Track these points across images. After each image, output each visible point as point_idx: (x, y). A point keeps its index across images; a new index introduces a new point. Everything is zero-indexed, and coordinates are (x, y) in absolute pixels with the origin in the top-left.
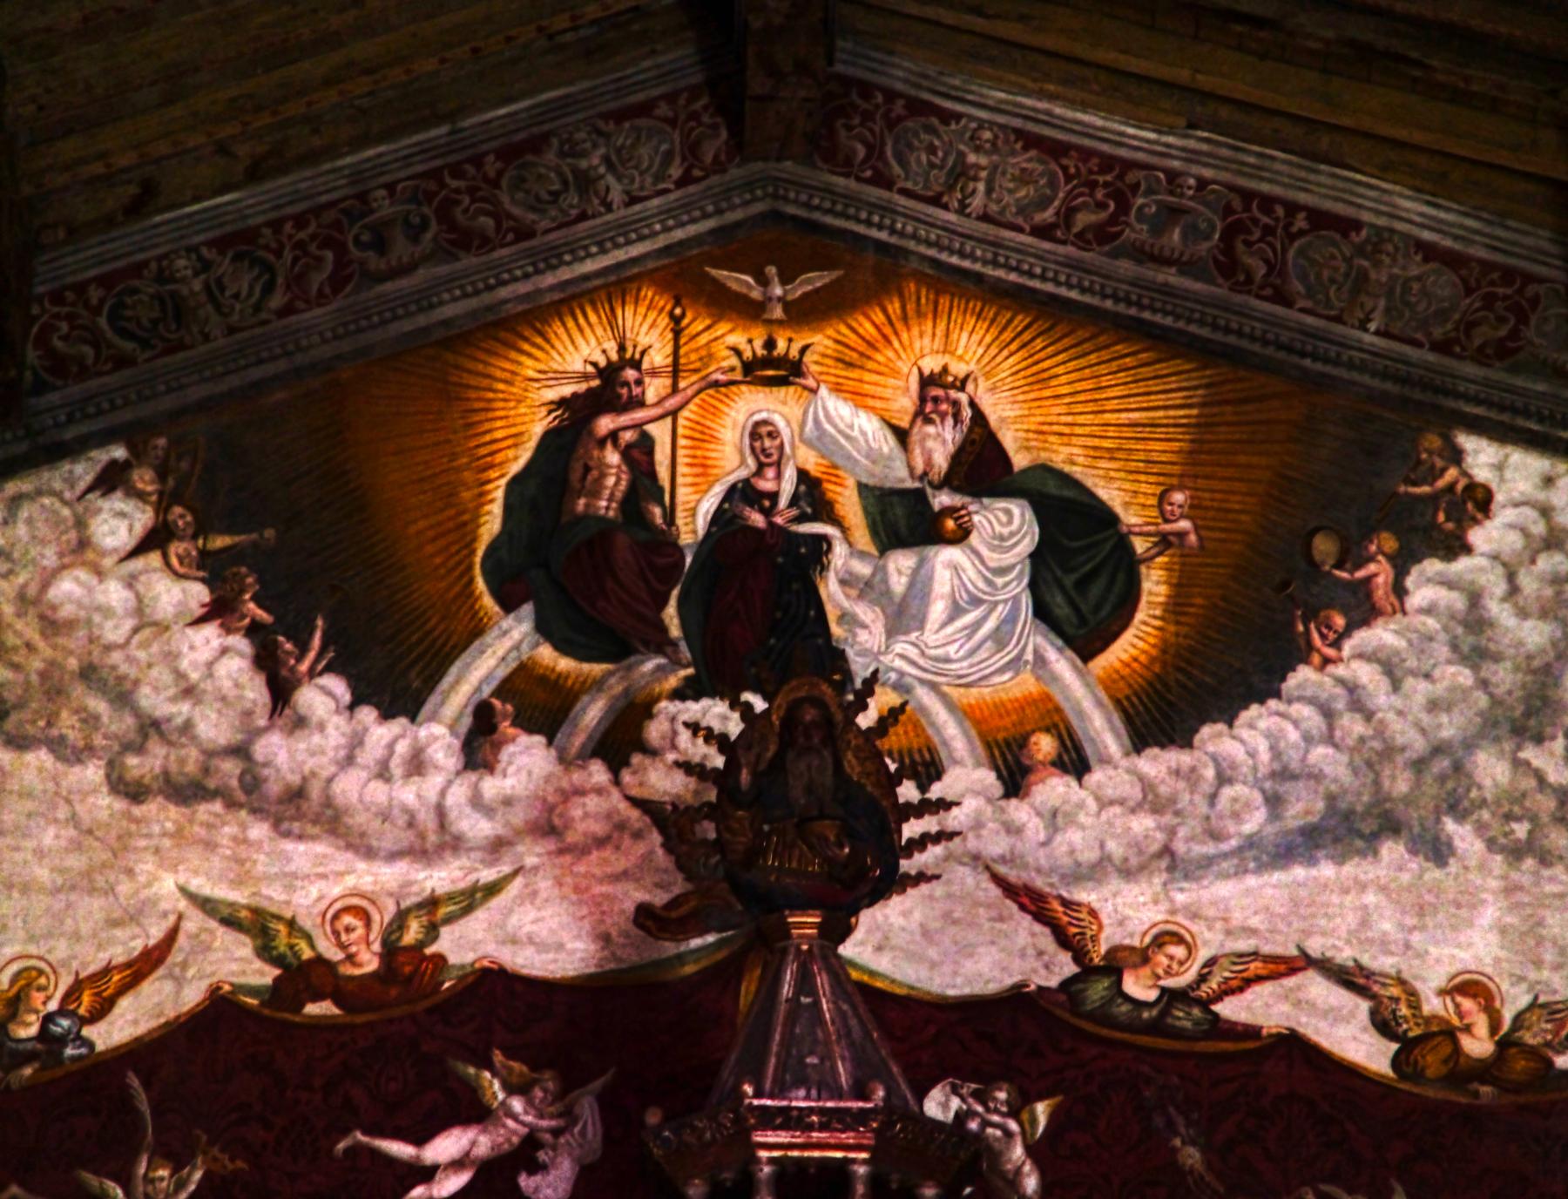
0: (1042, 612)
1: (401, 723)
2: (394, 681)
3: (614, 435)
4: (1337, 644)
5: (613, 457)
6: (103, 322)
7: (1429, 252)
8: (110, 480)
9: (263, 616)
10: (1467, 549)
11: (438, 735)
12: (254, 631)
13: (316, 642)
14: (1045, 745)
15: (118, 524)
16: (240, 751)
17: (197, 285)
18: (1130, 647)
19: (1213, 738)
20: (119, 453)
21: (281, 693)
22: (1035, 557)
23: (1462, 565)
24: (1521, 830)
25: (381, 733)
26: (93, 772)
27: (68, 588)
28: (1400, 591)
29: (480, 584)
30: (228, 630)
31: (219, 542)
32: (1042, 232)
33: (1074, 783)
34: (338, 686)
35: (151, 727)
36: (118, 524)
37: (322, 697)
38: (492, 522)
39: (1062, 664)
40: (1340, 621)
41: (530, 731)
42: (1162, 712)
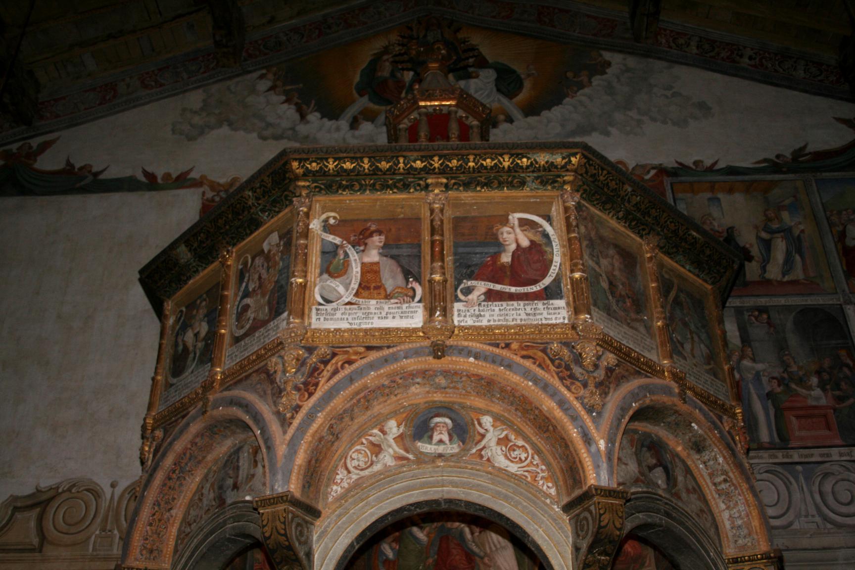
0: (499, 90)
1: (333, 122)
2: (331, 112)
3: (388, 60)
4: (576, 93)
5: (387, 64)
6: (262, 47)
7: (588, 16)
8: (262, 77)
9: (300, 101)
10: (606, 73)
11: (344, 124)
12: (296, 104)
13: (312, 105)
14: (502, 117)
15: (264, 85)
16: (293, 129)
17: (285, 38)
18: (521, 97)
19: (545, 113)
20: (264, 71)
21: (303, 117)
22: (497, 80)
23: (604, 77)
24: (628, 129)
25: (328, 123)
26: (255, 135)
27: (250, 100)
28: (590, 82)
29: (354, 92)
30: (290, 104)
31: (288, 88)
32: (494, 17)
33: (509, 124)
34: (318, 115)
35: (269, 125)
36: (264, 85)
37: (314, 117)
38: (357, 78)
39: (505, 101)
40: (575, 89)
41: (367, 120)
42: (531, 109)
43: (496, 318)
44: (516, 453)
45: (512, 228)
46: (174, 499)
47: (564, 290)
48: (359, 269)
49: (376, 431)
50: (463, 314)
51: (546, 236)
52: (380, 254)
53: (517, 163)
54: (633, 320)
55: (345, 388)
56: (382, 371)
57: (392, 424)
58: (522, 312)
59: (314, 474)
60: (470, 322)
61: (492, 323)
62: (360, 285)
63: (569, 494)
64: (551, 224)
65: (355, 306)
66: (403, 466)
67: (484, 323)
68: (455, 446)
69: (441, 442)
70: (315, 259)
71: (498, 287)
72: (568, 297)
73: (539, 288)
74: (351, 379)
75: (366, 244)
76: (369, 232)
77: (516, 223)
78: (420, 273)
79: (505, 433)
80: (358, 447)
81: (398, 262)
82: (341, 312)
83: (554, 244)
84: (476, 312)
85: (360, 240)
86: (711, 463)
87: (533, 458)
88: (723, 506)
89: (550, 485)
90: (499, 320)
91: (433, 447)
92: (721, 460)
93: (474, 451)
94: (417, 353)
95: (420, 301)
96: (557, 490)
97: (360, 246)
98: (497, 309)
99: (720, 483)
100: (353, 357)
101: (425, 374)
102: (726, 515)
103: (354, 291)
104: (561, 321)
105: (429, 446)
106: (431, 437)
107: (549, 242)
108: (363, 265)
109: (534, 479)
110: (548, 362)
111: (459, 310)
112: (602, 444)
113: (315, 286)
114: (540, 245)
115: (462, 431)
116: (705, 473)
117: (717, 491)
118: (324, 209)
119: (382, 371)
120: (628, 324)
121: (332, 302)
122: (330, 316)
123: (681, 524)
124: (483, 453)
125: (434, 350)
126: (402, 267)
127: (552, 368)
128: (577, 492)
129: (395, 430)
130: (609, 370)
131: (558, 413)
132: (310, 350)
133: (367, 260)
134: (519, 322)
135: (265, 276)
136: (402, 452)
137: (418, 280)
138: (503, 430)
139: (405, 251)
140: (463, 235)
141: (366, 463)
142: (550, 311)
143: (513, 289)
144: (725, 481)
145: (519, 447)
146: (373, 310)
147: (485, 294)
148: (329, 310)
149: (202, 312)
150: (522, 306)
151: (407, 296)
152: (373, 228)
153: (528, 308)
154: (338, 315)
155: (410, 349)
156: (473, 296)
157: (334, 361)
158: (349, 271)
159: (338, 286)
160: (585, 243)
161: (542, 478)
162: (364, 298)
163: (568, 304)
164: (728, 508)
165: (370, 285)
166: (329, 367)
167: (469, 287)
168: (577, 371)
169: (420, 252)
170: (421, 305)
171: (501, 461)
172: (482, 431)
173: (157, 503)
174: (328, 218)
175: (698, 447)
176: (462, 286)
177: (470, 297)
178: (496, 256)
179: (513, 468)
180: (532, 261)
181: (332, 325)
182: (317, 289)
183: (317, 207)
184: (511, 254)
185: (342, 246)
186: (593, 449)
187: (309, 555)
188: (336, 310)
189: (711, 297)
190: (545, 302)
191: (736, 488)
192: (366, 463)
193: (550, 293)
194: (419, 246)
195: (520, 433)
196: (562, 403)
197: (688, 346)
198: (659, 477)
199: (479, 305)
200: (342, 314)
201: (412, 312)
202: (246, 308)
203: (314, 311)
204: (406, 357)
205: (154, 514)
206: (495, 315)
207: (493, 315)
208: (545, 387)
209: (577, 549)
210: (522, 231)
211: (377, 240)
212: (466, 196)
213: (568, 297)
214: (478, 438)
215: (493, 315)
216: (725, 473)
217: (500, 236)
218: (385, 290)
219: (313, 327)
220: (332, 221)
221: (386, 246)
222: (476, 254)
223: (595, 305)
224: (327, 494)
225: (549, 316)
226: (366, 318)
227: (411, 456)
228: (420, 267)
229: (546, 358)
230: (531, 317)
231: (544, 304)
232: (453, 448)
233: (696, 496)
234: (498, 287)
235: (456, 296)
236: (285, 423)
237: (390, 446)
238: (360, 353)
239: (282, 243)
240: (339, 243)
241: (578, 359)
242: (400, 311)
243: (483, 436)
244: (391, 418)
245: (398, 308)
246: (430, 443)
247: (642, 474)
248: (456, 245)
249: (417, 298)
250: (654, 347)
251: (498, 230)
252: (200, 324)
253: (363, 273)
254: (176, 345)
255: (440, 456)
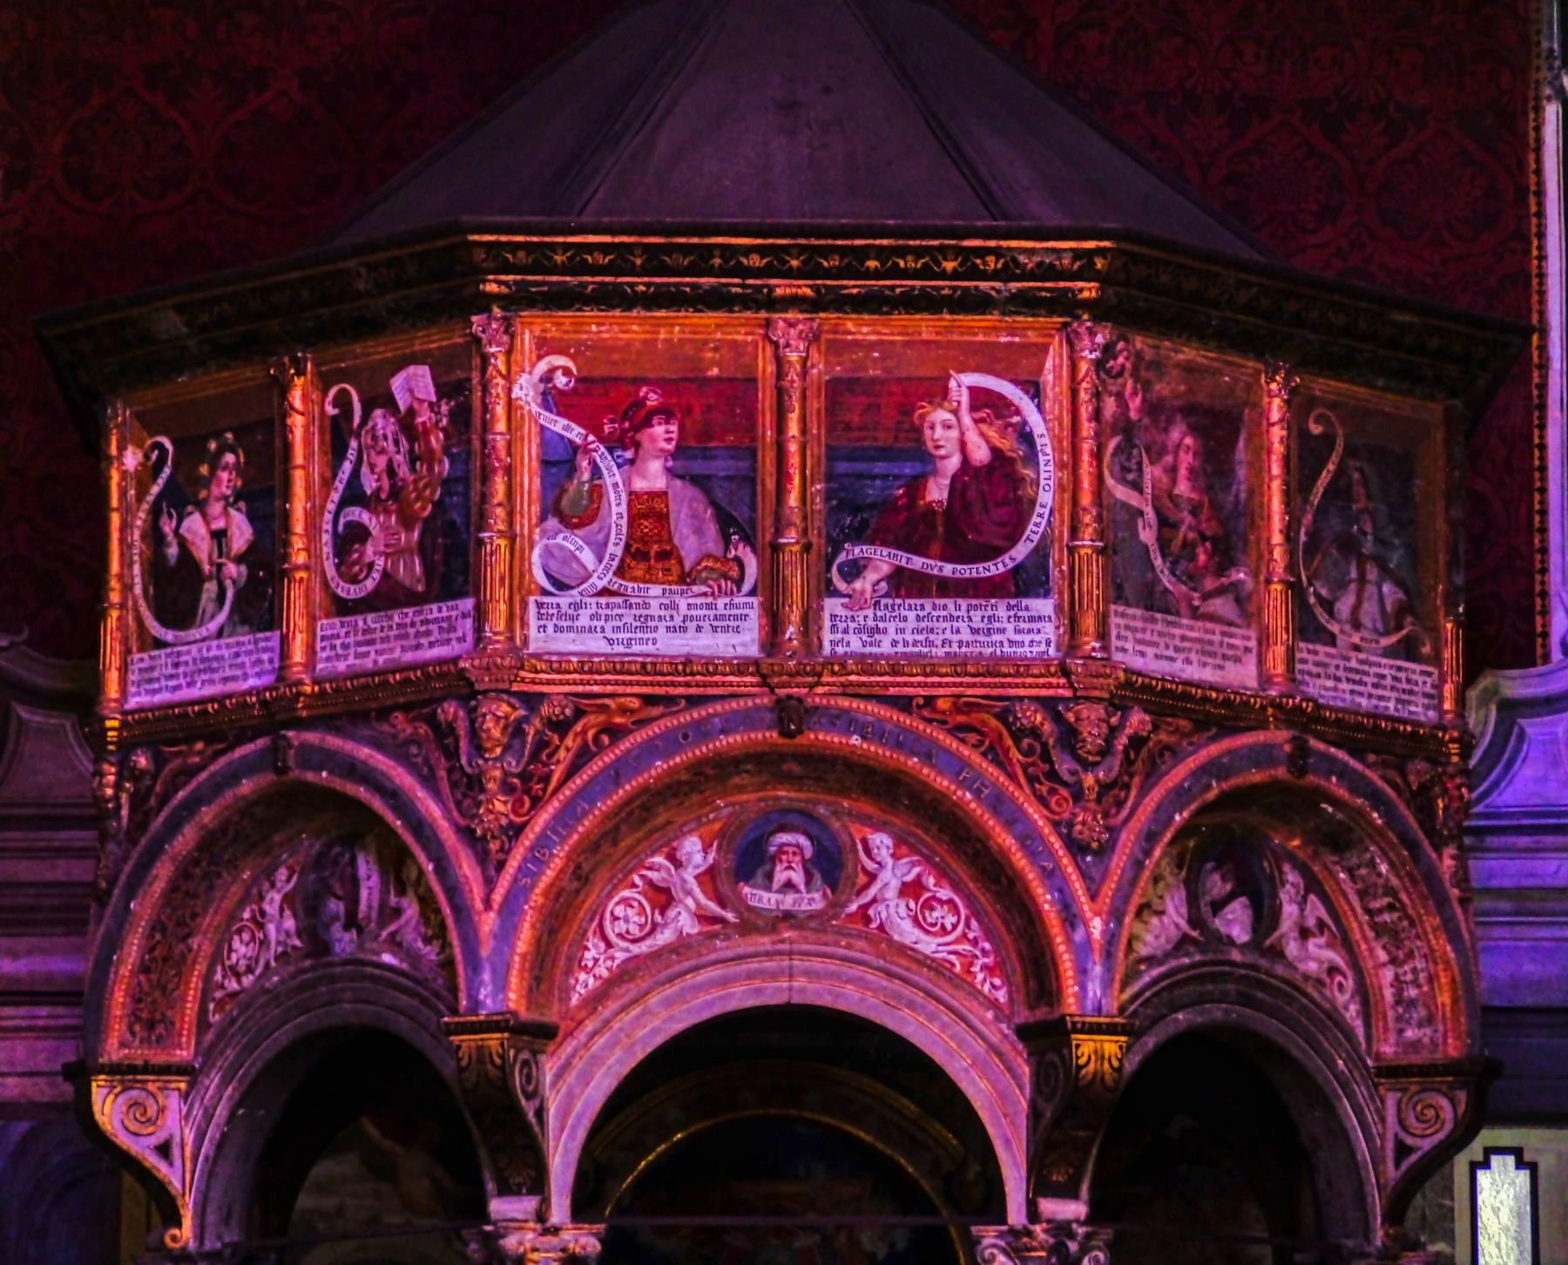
43: (909, 637)
44: (936, 914)
45: (955, 412)
46: (194, 916)
47: (1054, 573)
48: (624, 508)
49: (659, 859)
50: (842, 626)
51: (1027, 438)
52: (668, 470)
53: (976, 265)
54: (1206, 597)
55: (606, 794)
56: (678, 759)
57: (691, 846)
58: (962, 625)
59: (548, 965)
60: (855, 644)
61: (900, 649)
62: (627, 546)
63: (1031, 1008)
64: (1040, 407)
65: (619, 600)
66: (714, 935)
67: (886, 648)
68: (817, 896)
69: (789, 885)
70: (530, 480)
71: (918, 562)
72: (1061, 593)
73: (1001, 569)
74: (616, 774)
75: (637, 445)
76: (643, 413)
77: (965, 399)
78: (753, 522)
79: (917, 870)
80: (626, 893)
81: (707, 492)
82: (589, 612)
83: (1042, 458)
84: (873, 625)
85: (625, 442)
86: (1363, 871)
87: (968, 925)
88: (1383, 956)
89: (997, 982)
90: (915, 643)
91: (774, 897)
92: (1384, 868)
93: (853, 907)
94: (745, 720)
95: (752, 593)
96: (1010, 993)
97: (625, 449)
98: (911, 615)
99: (1380, 911)
100: (618, 720)
101: (764, 763)
102: (1388, 974)
103: (615, 563)
104: (1043, 648)
105: (765, 895)
106: (770, 876)
107: (1032, 457)
108: (633, 496)
109: (967, 968)
110: (1009, 742)
111: (833, 617)
112: (1097, 925)
113: (531, 548)
114: (1011, 461)
115: (831, 865)
116: (1349, 888)
117: (1374, 926)
118: (545, 347)
119: (678, 759)
120: (1195, 614)
121: (571, 588)
122: (566, 622)
123: (1271, 1012)
124: (871, 912)
125: (781, 720)
126: (714, 504)
127: (1015, 755)
128: (1042, 1013)
129: (698, 858)
130: (1137, 742)
131: (1020, 861)
132: (532, 701)
133: (639, 485)
134: (955, 648)
135: (403, 471)
136: (713, 907)
137: (749, 540)
138: (913, 864)
139: (721, 467)
140: (848, 427)
141: (642, 927)
142: (1022, 625)
143: (948, 569)
144: (1391, 908)
145: (941, 902)
146: (655, 610)
147: (889, 578)
148: (564, 609)
149: (226, 482)
150: (963, 613)
151: (726, 577)
152: (653, 400)
153: (976, 616)
154: (584, 621)
155: (734, 712)
156: (864, 584)
157: (578, 728)
158: (603, 511)
159: (580, 548)
160: (1112, 444)
161: (984, 967)
162: (634, 579)
163: (1058, 608)
164: (1394, 961)
165: (649, 551)
166: (569, 741)
167: (855, 561)
168: (1064, 766)
169: (754, 469)
170: (755, 601)
171: (906, 932)
172: (871, 866)
173: (157, 926)
174: (552, 370)
175: (1338, 839)
176: (842, 558)
177: (858, 585)
178: (916, 485)
179: (929, 945)
180: (996, 490)
181: (567, 643)
182: (536, 556)
183: (527, 339)
184: (947, 482)
185: (586, 450)
186: (1079, 936)
187: (540, 1113)
188: (577, 606)
189: (1439, 436)
190: (1013, 602)
191: (1412, 924)
192: (642, 927)
193: (1025, 582)
194: (753, 453)
195: (943, 875)
196: (1030, 840)
197: (1344, 606)
198: (1236, 922)
199: (877, 604)
200: (592, 617)
201: (736, 617)
202: (358, 534)
203: (532, 609)
204: (725, 731)
205: (153, 949)
206: (905, 631)
207: (903, 631)
208: (998, 803)
209: (1035, 1113)
210: (976, 421)
211: (661, 434)
212: (860, 328)
213: (1061, 593)
214: (862, 879)
215: (903, 631)
216: (1390, 891)
217: (928, 432)
218: (680, 562)
219: (532, 648)
220: (561, 381)
221: (680, 452)
222: (874, 477)
223: (1119, 596)
224: (567, 992)
225: (1018, 638)
226: (642, 629)
227: (730, 916)
228: (753, 509)
229: (1005, 733)
230: (981, 638)
231: (1009, 607)
232: (813, 901)
233: (1322, 940)
234: (918, 562)
235: (829, 582)
236: (491, 866)
237: (689, 893)
238: (632, 712)
239: (444, 409)
240: (578, 441)
241: (1070, 737)
242: (712, 613)
243: (872, 877)
244: (690, 832)
245: (709, 606)
246: (768, 889)
247: (1195, 920)
248: (833, 454)
249: (746, 587)
250: (1253, 644)
251: (922, 417)
252: (226, 513)
253: (634, 518)
254: (155, 537)
255: (788, 916)
